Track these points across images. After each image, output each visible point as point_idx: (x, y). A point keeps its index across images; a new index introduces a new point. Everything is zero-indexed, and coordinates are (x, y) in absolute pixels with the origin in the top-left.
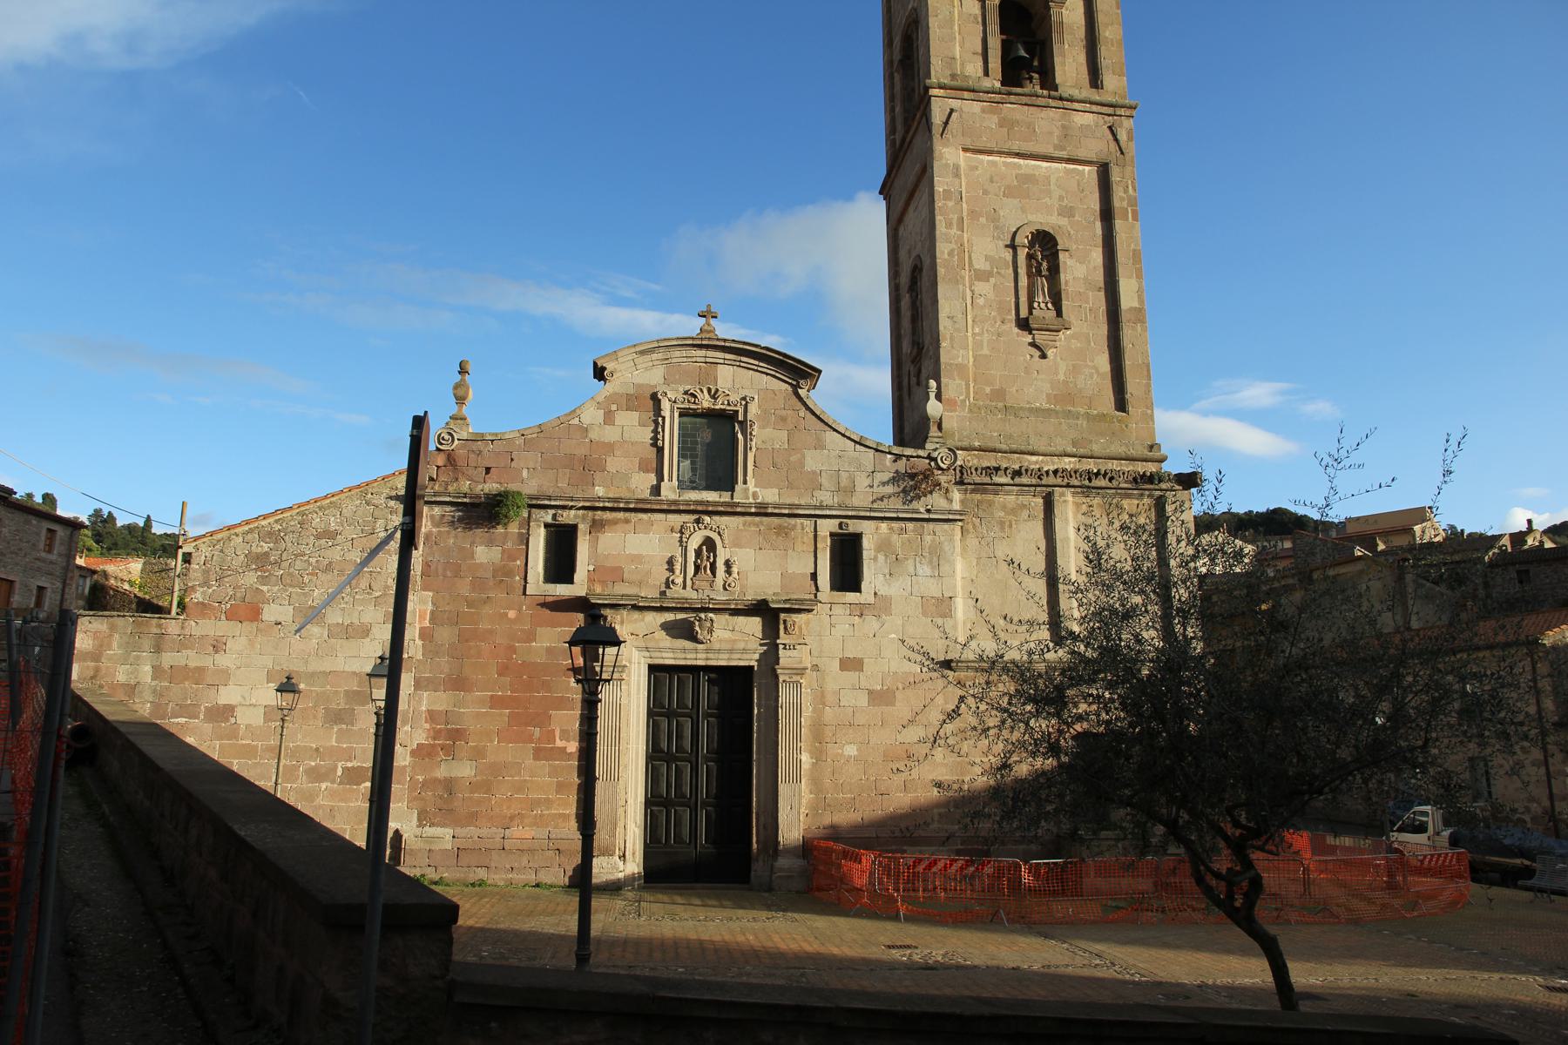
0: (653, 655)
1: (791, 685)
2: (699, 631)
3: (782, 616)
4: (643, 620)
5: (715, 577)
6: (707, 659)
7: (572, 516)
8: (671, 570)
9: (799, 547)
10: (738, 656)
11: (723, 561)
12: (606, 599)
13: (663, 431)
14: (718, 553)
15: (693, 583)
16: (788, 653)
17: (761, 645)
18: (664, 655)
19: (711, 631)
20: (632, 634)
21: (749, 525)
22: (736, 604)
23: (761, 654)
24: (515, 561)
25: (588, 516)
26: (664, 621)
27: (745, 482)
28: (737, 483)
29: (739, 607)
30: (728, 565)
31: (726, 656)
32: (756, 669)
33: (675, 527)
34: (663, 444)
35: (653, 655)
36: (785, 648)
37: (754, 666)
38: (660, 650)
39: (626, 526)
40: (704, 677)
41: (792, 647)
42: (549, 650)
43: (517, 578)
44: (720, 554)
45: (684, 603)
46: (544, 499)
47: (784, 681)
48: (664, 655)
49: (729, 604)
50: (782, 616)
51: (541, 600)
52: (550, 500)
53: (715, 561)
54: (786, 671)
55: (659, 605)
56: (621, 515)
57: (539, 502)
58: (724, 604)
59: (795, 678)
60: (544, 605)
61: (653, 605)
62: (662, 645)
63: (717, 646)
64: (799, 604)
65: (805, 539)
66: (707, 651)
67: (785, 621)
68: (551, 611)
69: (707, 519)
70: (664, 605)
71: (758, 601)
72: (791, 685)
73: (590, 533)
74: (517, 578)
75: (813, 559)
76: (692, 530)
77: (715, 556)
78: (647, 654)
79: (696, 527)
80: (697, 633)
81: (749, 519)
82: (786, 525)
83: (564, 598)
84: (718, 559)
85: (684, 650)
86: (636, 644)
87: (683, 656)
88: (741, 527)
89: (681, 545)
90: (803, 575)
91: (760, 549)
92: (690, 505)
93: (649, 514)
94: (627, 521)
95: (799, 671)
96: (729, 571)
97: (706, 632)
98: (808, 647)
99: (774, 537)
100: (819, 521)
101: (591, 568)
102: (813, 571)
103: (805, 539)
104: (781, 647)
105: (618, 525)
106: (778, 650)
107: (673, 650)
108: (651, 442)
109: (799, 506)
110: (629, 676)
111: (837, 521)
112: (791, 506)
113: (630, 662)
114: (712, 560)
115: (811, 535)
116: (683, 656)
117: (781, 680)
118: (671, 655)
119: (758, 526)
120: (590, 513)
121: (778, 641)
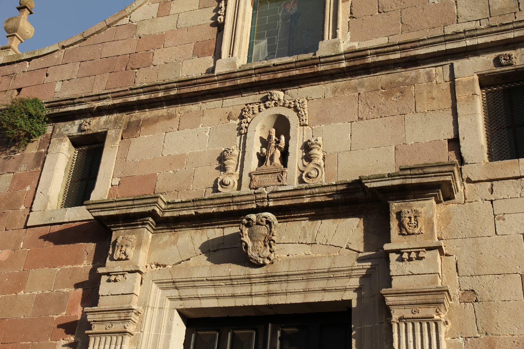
0: (185, 293)
1: (418, 325)
2: (250, 244)
3: (395, 206)
4: (175, 243)
5: (285, 166)
6: (269, 294)
7: (102, 123)
8: (223, 168)
9: (424, 105)
10: (322, 284)
11: (301, 144)
12: (111, 208)
13: (226, 6)
14: (291, 133)
15: (251, 180)
16: (408, 267)
17: (360, 260)
18: (201, 292)
19: (269, 242)
20: (157, 265)
21: (343, 90)
22: (313, 195)
23: (363, 278)
24: (24, 187)
25: (121, 119)
26: (206, 240)
27: (335, 36)
28: (323, 39)
29: (318, 199)
30: (307, 147)
31: (299, 286)
32: (354, 304)
33: (234, 113)
34: (224, 19)
35: (185, 293)
36: (400, 259)
37: (350, 301)
38: (194, 283)
39: (169, 123)
40: (274, 334)
41: (413, 255)
42: (40, 301)
43: (23, 207)
44: (295, 136)
45: (229, 204)
46: (67, 105)
47: (401, 319)
48: (201, 292)
49: (300, 196)
50: (395, 206)
51: (47, 230)
52: (74, 104)
53: (287, 145)
54: (405, 299)
55: (193, 212)
56: (163, 111)
57: (62, 110)
58: (293, 197)
59: (423, 312)
60: (47, 237)
61: (185, 213)
62: (197, 274)
63: (282, 269)
64: (419, 176)
65: (435, 93)
66: (269, 279)
67: (399, 215)
68: (56, 243)
69: (278, 94)
70: (201, 211)
71: (348, 184)
72: (418, 325)
73: (122, 138)
74: (23, 207)
75: (451, 119)
76: (256, 111)
77: (287, 139)
78: (175, 293)
79: (262, 107)
80: (246, 247)
81: (340, 83)
82: (401, 79)
83: (73, 225)
84: (291, 142)
85: (231, 281)
86: (157, 277)
87: (229, 291)
88: (329, 95)
89: (240, 134)
90: (434, 143)
91: (360, 119)
92: (250, 75)
93: (200, 104)
94: (170, 117)
95: (430, 298)
96: (308, 158)
97: (261, 244)
98: (452, 260)
99: (383, 100)
100: (457, 64)
101: (116, 182)
102: (451, 136)
103: (435, 93)
104: (393, 257)
105: (158, 124)
106: (388, 261)
107: (213, 282)
108: (212, 22)
109: (415, 44)
110: (140, 328)
111: (490, 57)
112: (403, 46)
113: (145, 306)
114: (282, 144)
115: (446, 86)
116: (229, 291)
117: (396, 315)
118: (211, 292)
119: (355, 89)
120: (125, 117)
121: (387, 247)
